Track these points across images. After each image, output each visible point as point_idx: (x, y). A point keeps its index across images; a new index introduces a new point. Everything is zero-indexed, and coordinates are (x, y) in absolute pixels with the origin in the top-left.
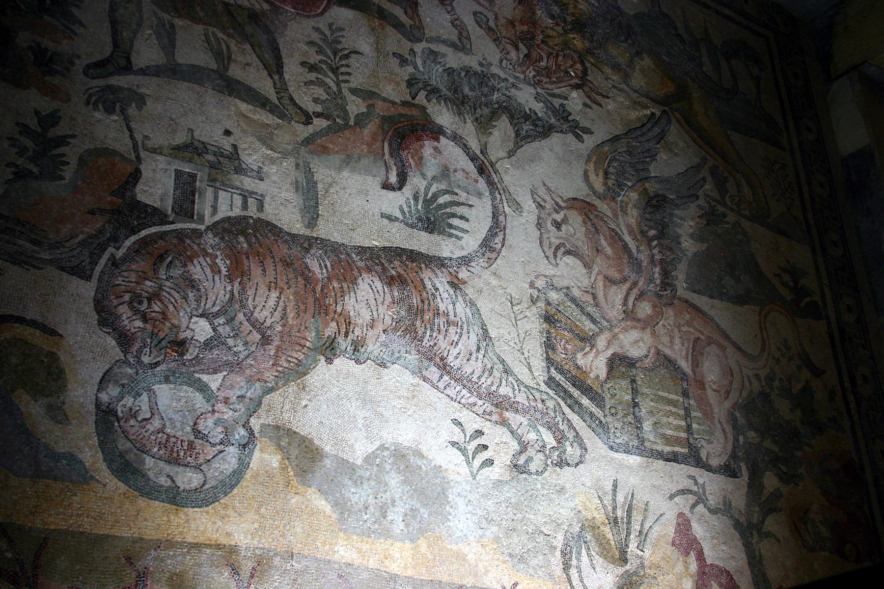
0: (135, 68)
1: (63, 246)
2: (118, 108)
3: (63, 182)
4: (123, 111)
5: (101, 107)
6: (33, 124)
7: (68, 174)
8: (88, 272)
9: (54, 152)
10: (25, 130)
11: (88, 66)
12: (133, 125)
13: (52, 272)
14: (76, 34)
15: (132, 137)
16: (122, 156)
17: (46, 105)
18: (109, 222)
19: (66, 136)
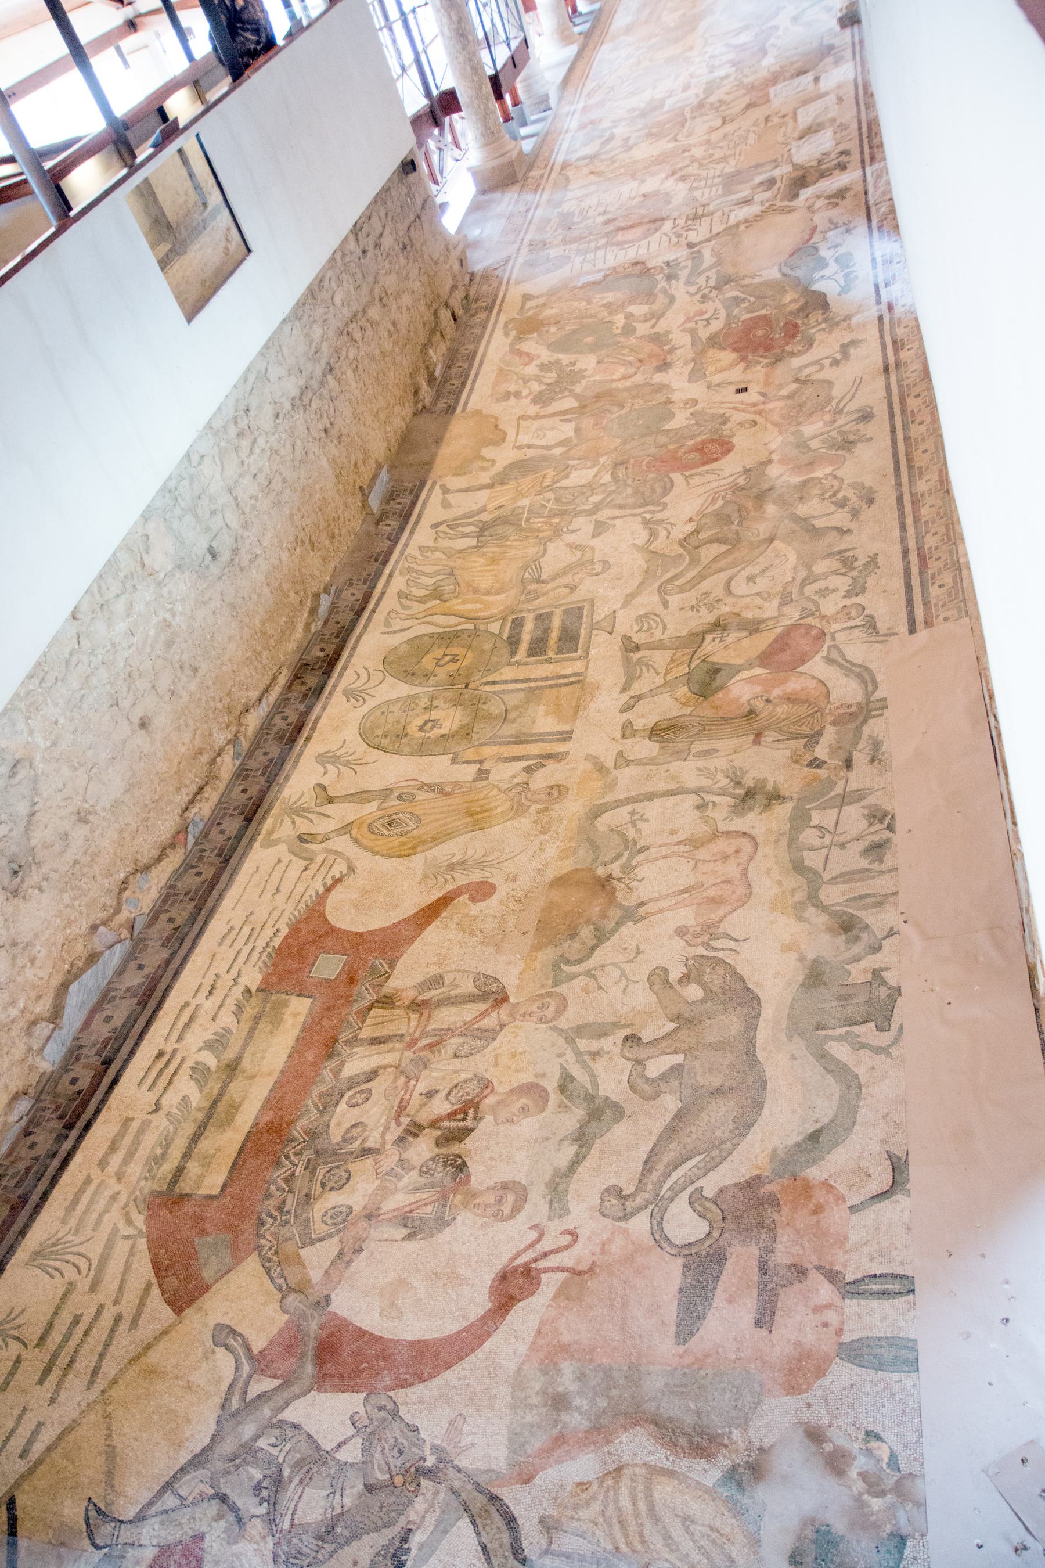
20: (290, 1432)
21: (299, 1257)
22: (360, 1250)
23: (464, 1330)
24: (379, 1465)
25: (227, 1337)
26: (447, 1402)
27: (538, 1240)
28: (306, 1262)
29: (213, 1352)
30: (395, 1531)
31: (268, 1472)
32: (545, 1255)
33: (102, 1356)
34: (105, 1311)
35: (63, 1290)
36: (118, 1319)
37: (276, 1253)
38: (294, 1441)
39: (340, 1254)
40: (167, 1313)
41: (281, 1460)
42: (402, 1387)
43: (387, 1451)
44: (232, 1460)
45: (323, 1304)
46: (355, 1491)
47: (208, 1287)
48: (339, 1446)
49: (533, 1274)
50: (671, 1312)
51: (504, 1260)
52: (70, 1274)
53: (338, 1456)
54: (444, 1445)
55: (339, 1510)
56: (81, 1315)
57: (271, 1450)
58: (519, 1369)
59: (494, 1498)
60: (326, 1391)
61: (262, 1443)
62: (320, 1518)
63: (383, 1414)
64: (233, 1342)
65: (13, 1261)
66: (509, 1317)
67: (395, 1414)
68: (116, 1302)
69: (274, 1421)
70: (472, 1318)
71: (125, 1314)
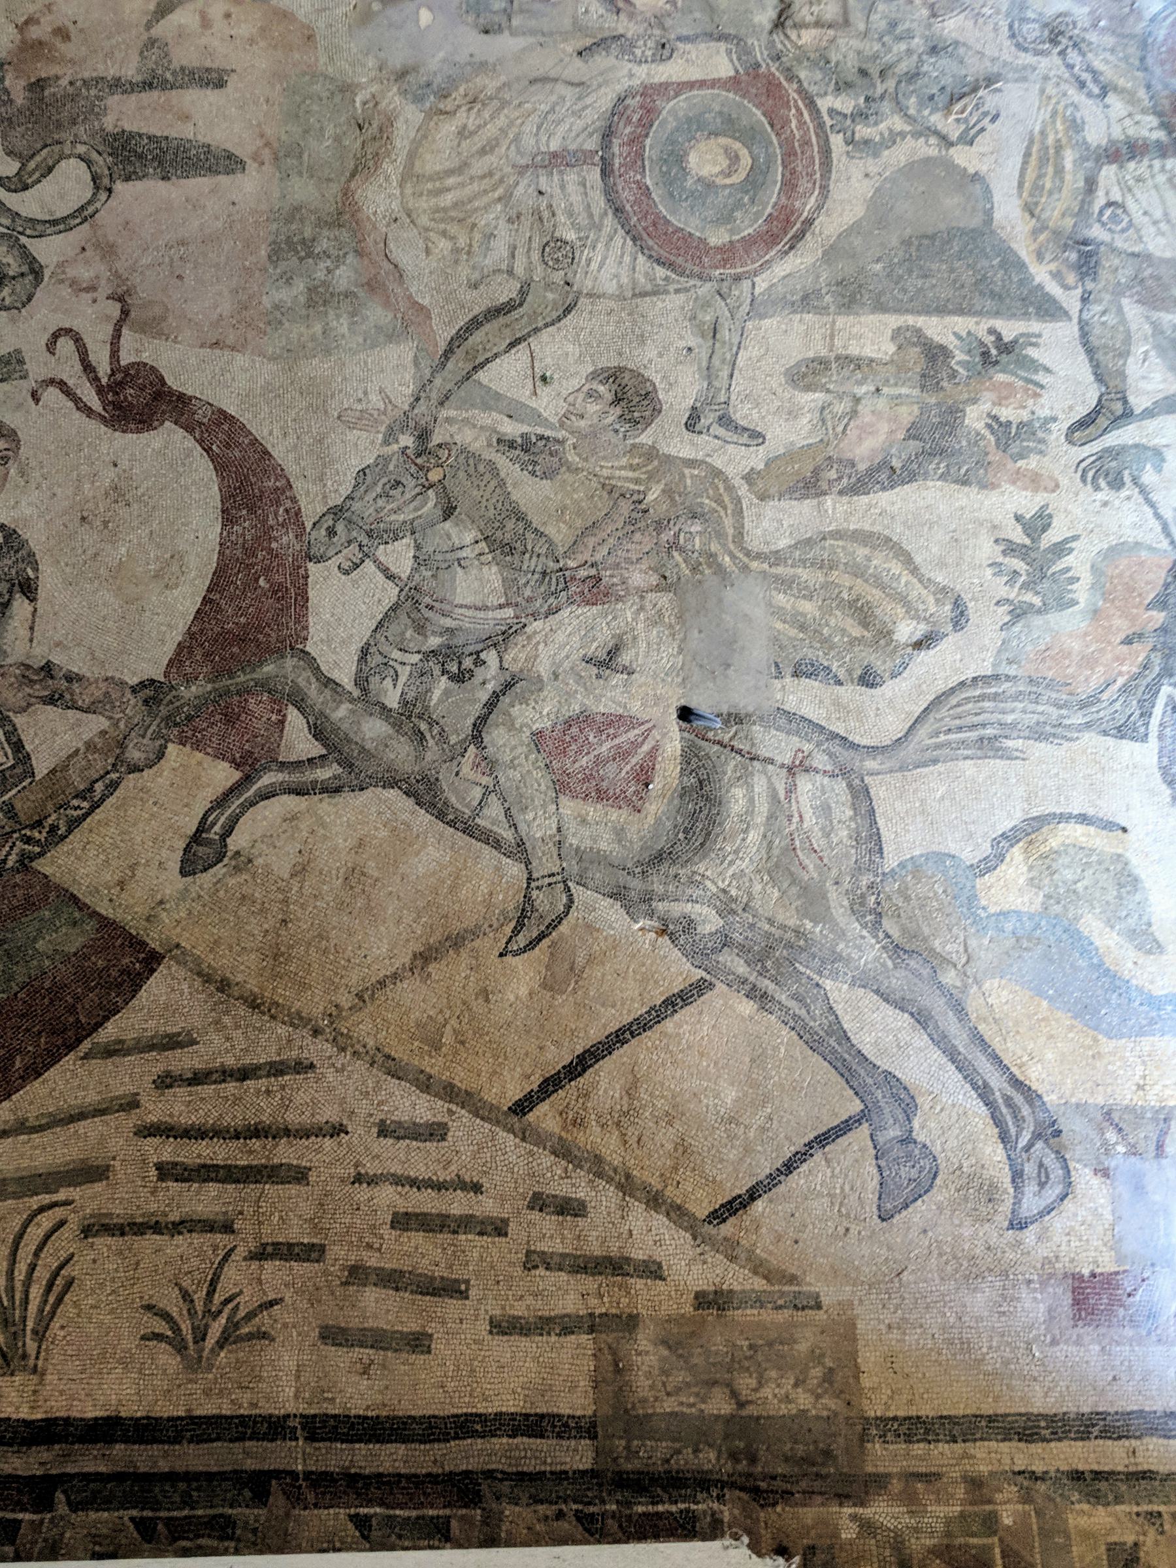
0: (1137, 411)
1: (1099, 701)
2: (1127, 478)
3: (1076, 608)
4: (1135, 481)
5: (1102, 483)
6: (1018, 535)
7: (1082, 593)
8: (1142, 730)
9: (1054, 569)
10: (1011, 549)
11: (1072, 429)
12: (1154, 497)
13: (1091, 740)
14: (1042, 387)
15: (1158, 516)
16: (1150, 548)
17: (1027, 502)
18: (1154, 649)
19: (1066, 541)
20: (374, 660)
21: (53, 771)
22: (48, 669)
23: (208, 450)
24: (416, 509)
25: (209, 842)
26: (320, 441)
27: (62, 385)
28: (64, 754)
29: (237, 853)
30: (502, 462)
31: (437, 671)
32: (88, 368)
33: (244, 1074)
34: (152, 1118)
35: (103, 1242)
36: (165, 1082)
37: (39, 824)
38: (385, 648)
39: (51, 700)
40: (156, 988)
41: (416, 658)
42: (298, 513)
43: (393, 505)
44: (422, 737)
45: (149, 692)
46: (454, 532)
47: (105, 923)
48: (390, 577)
49: (119, 377)
50: (199, 184)
51: (95, 427)
52: (65, 1241)
53: (404, 576)
54: (383, 429)
55: (483, 545)
56: (159, 1167)
57: (402, 679)
58: (274, 358)
59: (448, 353)
60: (306, 628)
61: (392, 700)
62: (494, 569)
63: (340, 527)
64: (217, 828)
65: (25, 1414)
66: (190, 392)
67: (337, 512)
68: (131, 1104)
69: (356, 693)
70: (190, 443)
71: (158, 1069)
